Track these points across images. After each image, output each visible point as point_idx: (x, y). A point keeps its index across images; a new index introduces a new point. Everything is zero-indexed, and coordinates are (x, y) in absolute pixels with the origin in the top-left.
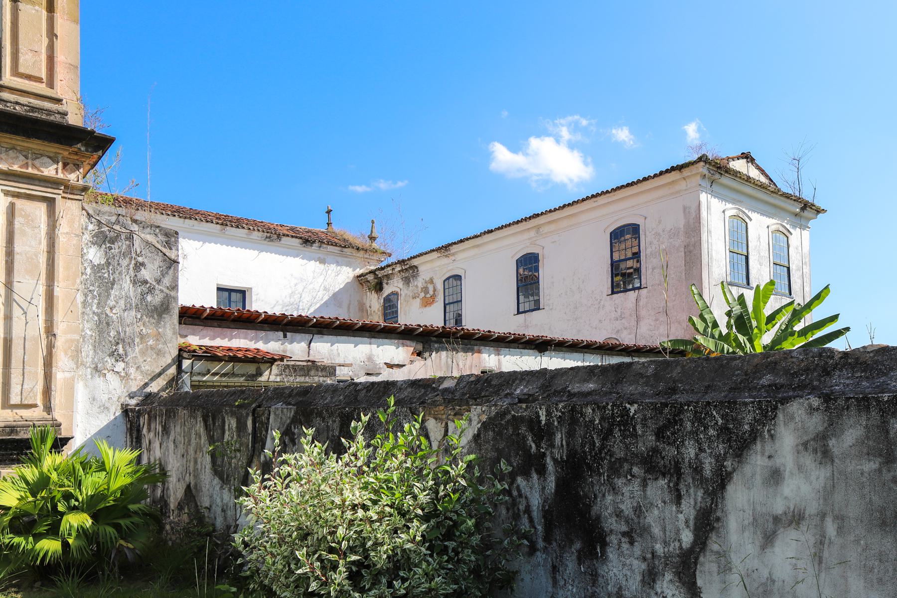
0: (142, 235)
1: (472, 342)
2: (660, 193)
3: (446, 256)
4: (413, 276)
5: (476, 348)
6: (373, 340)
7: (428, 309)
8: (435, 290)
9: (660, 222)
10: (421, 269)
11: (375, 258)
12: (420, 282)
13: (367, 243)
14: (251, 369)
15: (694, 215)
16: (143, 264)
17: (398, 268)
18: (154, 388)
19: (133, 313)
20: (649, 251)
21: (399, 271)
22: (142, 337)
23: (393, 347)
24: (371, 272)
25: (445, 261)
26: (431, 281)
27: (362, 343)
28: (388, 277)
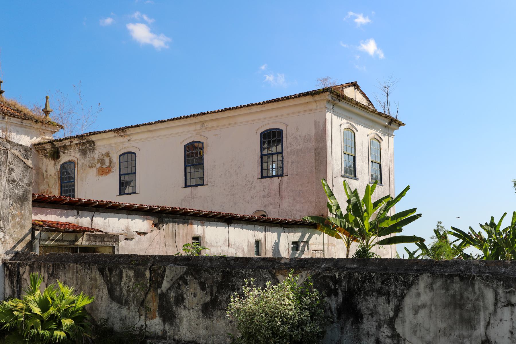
0: (13, 151)
1: (187, 217)
2: (298, 109)
3: (122, 136)
4: (90, 149)
5: (190, 221)
6: (129, 216)
7: (104, 177)
8: (111, 162)
9: (297, 130)
10: (98, 144)
11: (49, 129)
12: (96, 155)
13: (42, 115)
14: (72, 237)
15: (321, 128)
16: (13, 169)
17: (76, 141)
18: (19, 248)
19: (8, 201)
20: (289, 149)
21: (77, 144)
22: (13, 216)
23: (141, 221)
24: (48, 142)
25: (120, 139)
26: (108, 155)
27: (123, 218)
28: (65, 147)
